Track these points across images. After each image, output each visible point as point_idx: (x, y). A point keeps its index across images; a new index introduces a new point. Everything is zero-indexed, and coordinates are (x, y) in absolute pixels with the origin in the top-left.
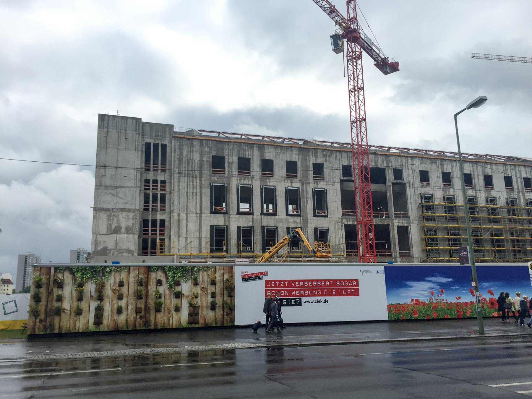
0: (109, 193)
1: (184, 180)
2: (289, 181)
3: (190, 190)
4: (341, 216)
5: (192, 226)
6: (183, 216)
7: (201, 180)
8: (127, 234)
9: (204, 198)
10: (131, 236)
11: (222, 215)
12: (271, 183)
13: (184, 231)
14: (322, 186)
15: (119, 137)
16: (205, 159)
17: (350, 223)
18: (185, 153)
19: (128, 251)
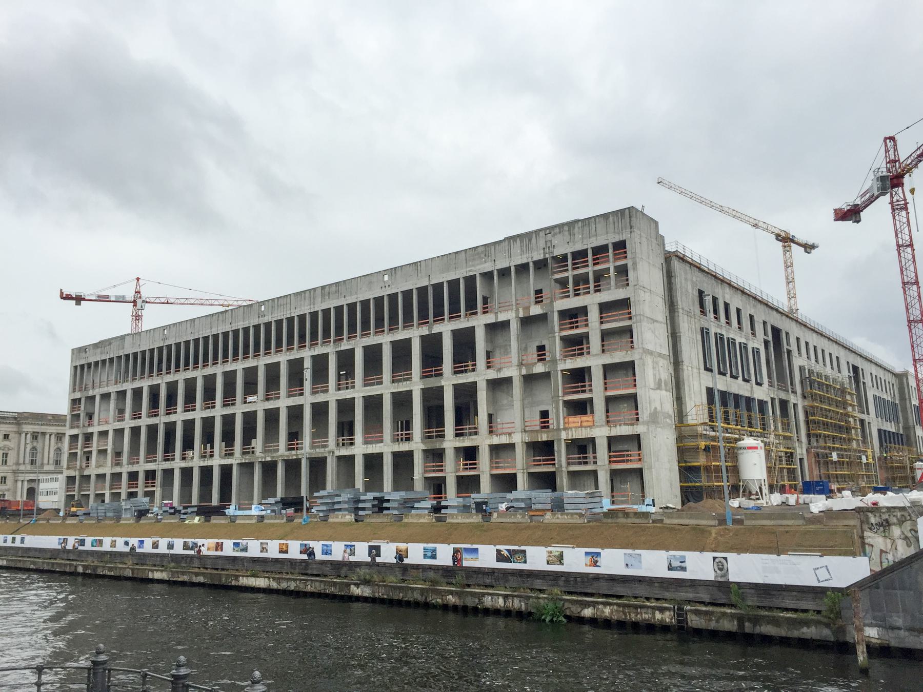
0: (650, 329)
1: (686, 317)
2: (740, 335)
3: (690, 335)
4: (767, 386)
5: (696, 384)
6: (690, 368)
7: (695, 321)
8: (666, 390)
9: (699, 348)
10: (668, 393)
11: (709, 373)
12: (731, 336)
13: (693, 391)
14: (756, 346)
15: (648, 248)
16: (694, 293)
17: (772, 396)
18: (683, 281)
19: (669, 416)
